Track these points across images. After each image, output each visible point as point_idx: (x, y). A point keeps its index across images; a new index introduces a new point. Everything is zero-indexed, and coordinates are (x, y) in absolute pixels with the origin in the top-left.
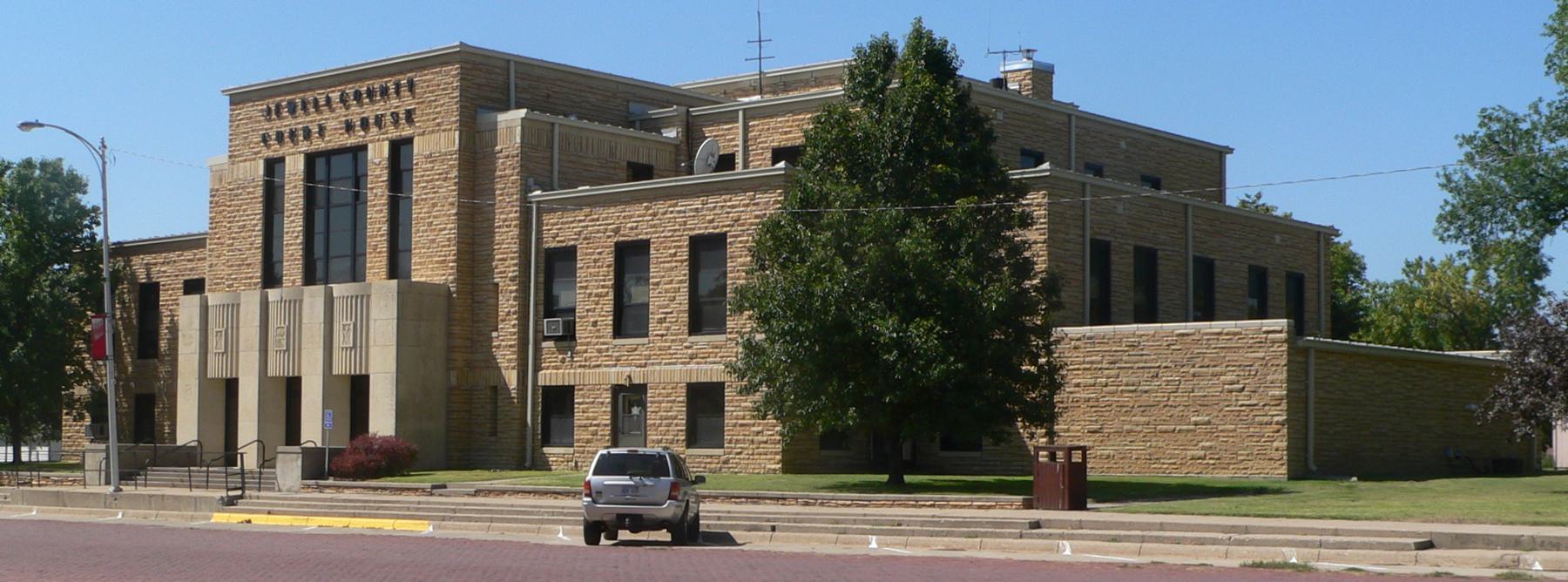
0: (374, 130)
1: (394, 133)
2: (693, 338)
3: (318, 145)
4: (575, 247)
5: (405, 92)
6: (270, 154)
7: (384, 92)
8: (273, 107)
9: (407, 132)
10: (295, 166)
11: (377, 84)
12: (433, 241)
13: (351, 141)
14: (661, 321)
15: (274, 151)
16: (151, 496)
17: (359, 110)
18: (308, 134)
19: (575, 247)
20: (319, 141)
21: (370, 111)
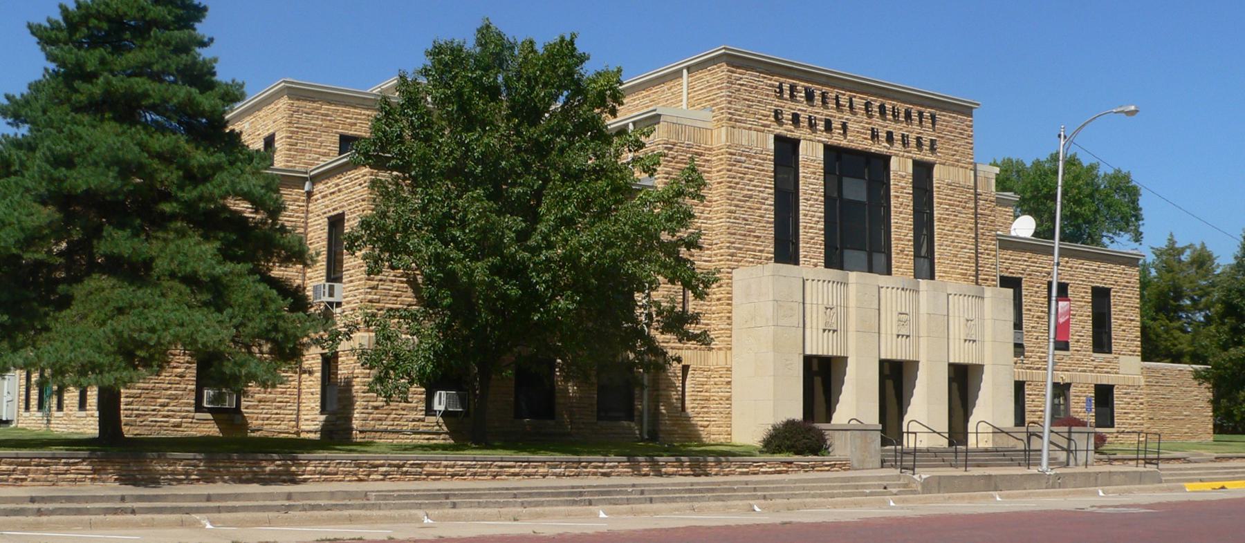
0: (898, 145)
1: (918, 157)
2: (1096, 355)
3: (837, 139)
4: (1020, 279)
5: (927, 123)
6: (781, 131)
7: (908, 115)
8: (786, 87)
9: (929, 158)
10: (811, 154)
11: (902, 107)
12: (955, 256)
13: (875, 148)
14: (1078, 341)
15: (787, 130)
16: (1097, 473)
17: (881, 122)
18: (828, 127)
19: (1020, 279)
20: (842, 138)
21: (898, 129)
